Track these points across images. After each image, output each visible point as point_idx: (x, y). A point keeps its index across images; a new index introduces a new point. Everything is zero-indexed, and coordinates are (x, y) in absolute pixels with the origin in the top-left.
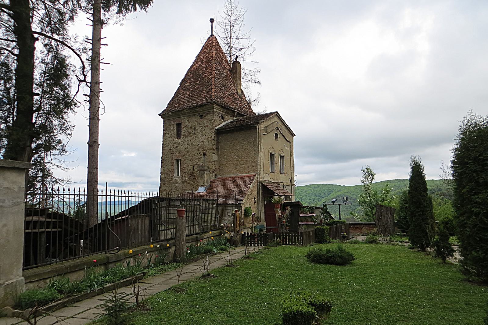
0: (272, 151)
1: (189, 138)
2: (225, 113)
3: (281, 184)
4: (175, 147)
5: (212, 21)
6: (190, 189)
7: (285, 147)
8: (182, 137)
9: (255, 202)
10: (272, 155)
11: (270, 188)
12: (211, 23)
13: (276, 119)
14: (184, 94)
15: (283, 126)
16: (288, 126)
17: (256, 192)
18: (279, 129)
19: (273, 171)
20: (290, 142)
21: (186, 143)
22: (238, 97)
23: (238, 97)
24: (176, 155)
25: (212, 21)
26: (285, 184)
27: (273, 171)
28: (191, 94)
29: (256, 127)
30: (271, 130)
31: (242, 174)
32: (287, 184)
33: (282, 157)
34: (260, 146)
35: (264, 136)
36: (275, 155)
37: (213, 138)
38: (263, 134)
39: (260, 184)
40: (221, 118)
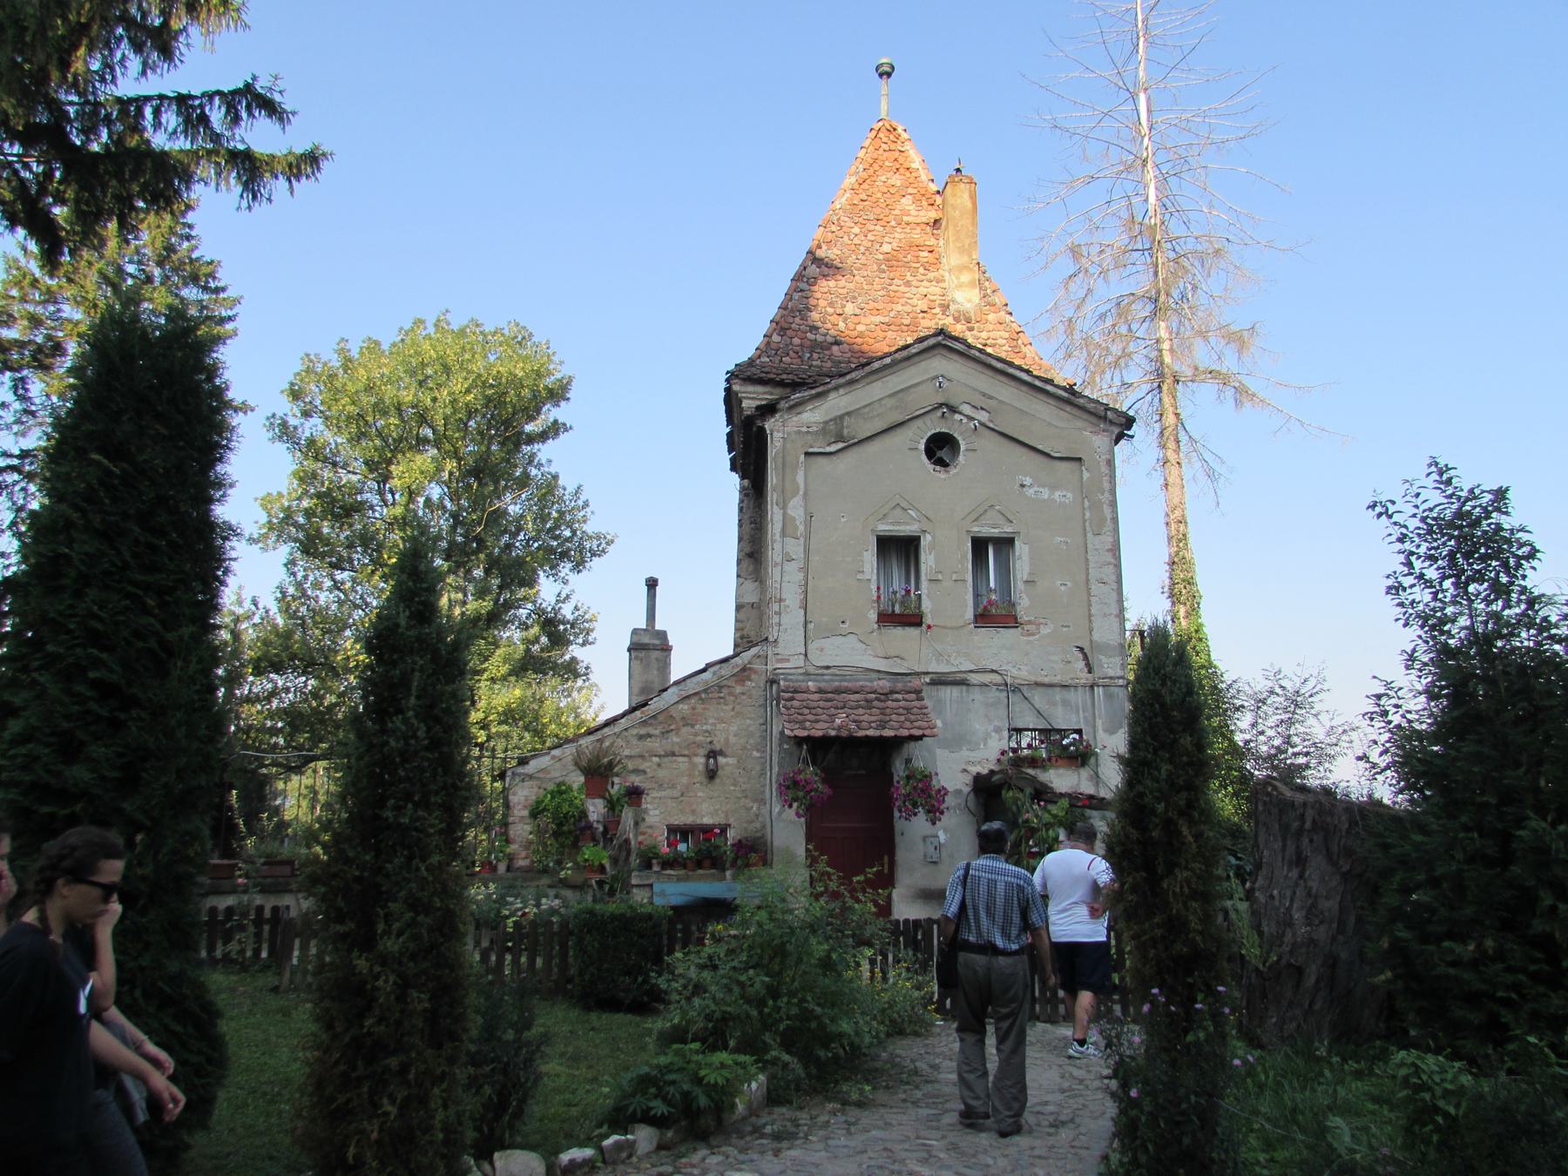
0: (893, 524)
3: (975, 678)
7: (1030, 492)
9: (711, 774)
10: (899, 550)
13: (941, 364)
15: (1006, 392)
16: (1050, 381)
18: (966, 409)
20: (1080, 459)
26: (1021, 672)
27: (902, 616)
29: (762, 430)
30: (880, 425)
32: (1046, 680)
34: (784, 508)
35: (820, 460)
36: (925, 541)
38: (807, 454)
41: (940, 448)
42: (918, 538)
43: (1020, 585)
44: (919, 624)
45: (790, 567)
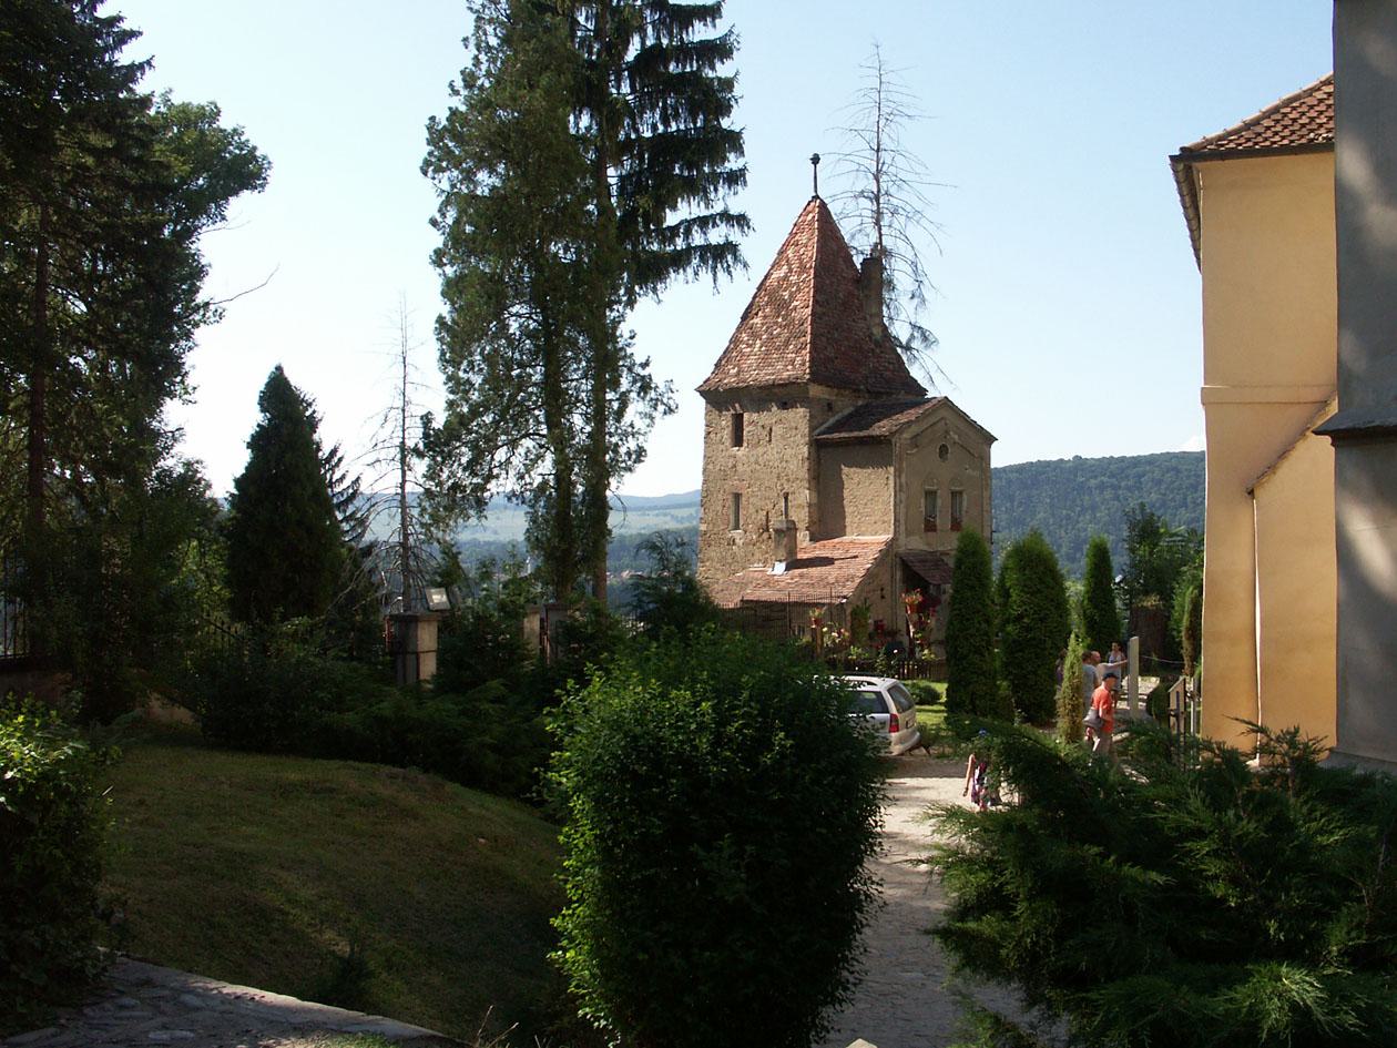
1: (760, 450)
2: (837, 395)
4: (730, 465)
5: (816, 160)
6: (760, 560)
8: (745, 444)
9: (883, 597)
10: (930, 495)
11: (917, 568)
12: (813, 166)
14: (749, 346)
17: (888, 576)
19: (930, 527)
21: (752, 460)
22: (873, 346)
23: (873, 346)
24: (733, 484)
25: (816, 160)
27: (930, 527)
28: (763, 349)
31: (863, 535)
33: (954, 494)
37: (806, 455)
39: (898, 559)
40: (826, 408)
41: (943, 451)
42: (936, 492)
43: (963, 513)
44: (935, 530)
45: (902, 505)
